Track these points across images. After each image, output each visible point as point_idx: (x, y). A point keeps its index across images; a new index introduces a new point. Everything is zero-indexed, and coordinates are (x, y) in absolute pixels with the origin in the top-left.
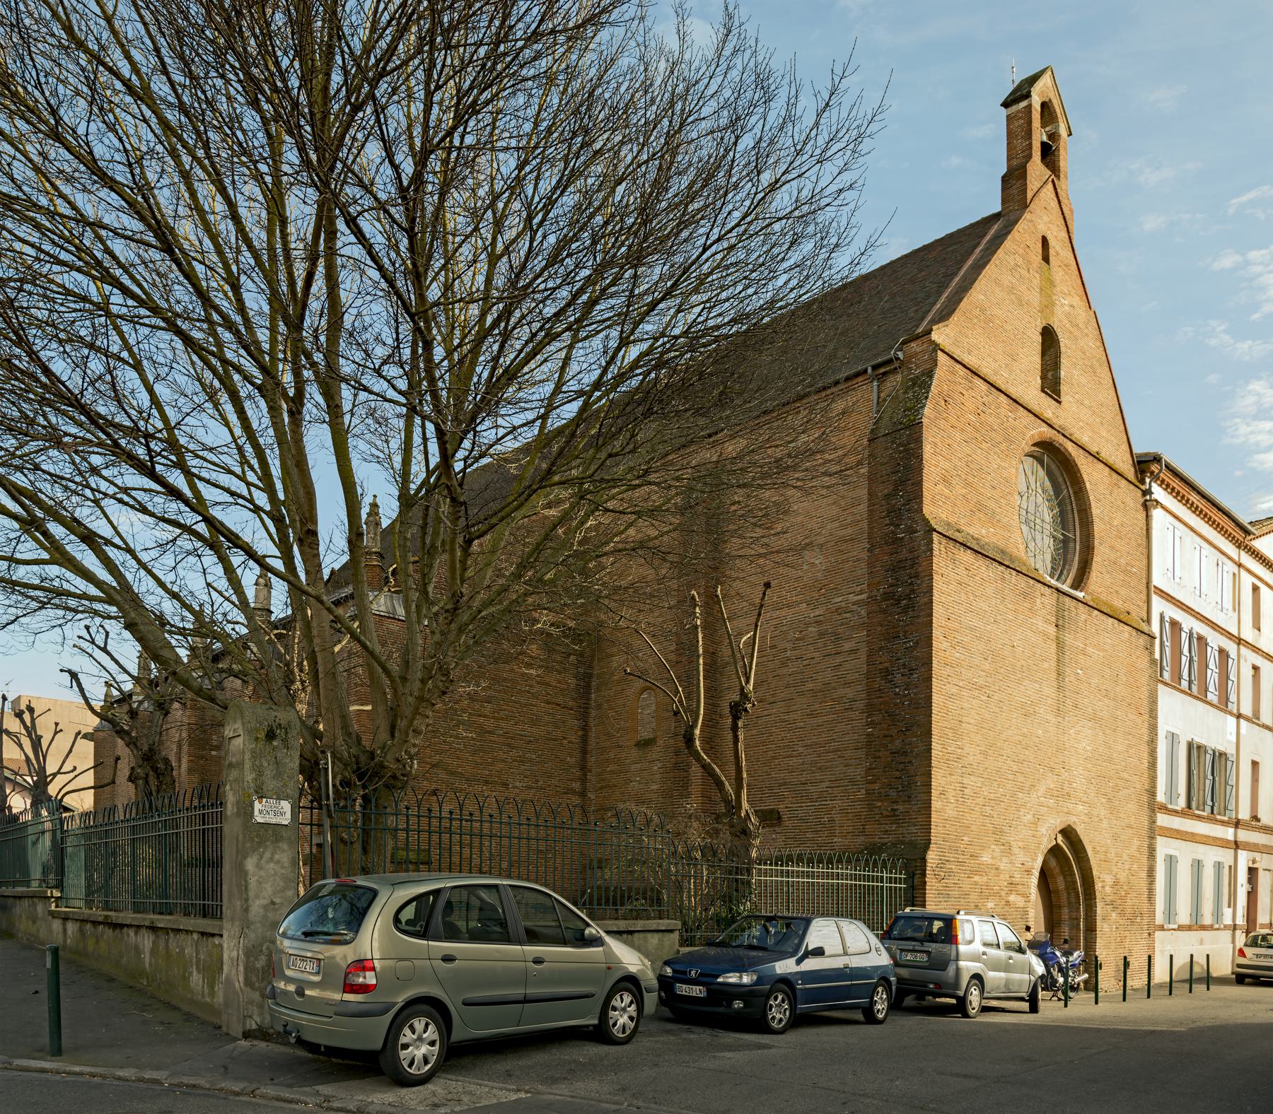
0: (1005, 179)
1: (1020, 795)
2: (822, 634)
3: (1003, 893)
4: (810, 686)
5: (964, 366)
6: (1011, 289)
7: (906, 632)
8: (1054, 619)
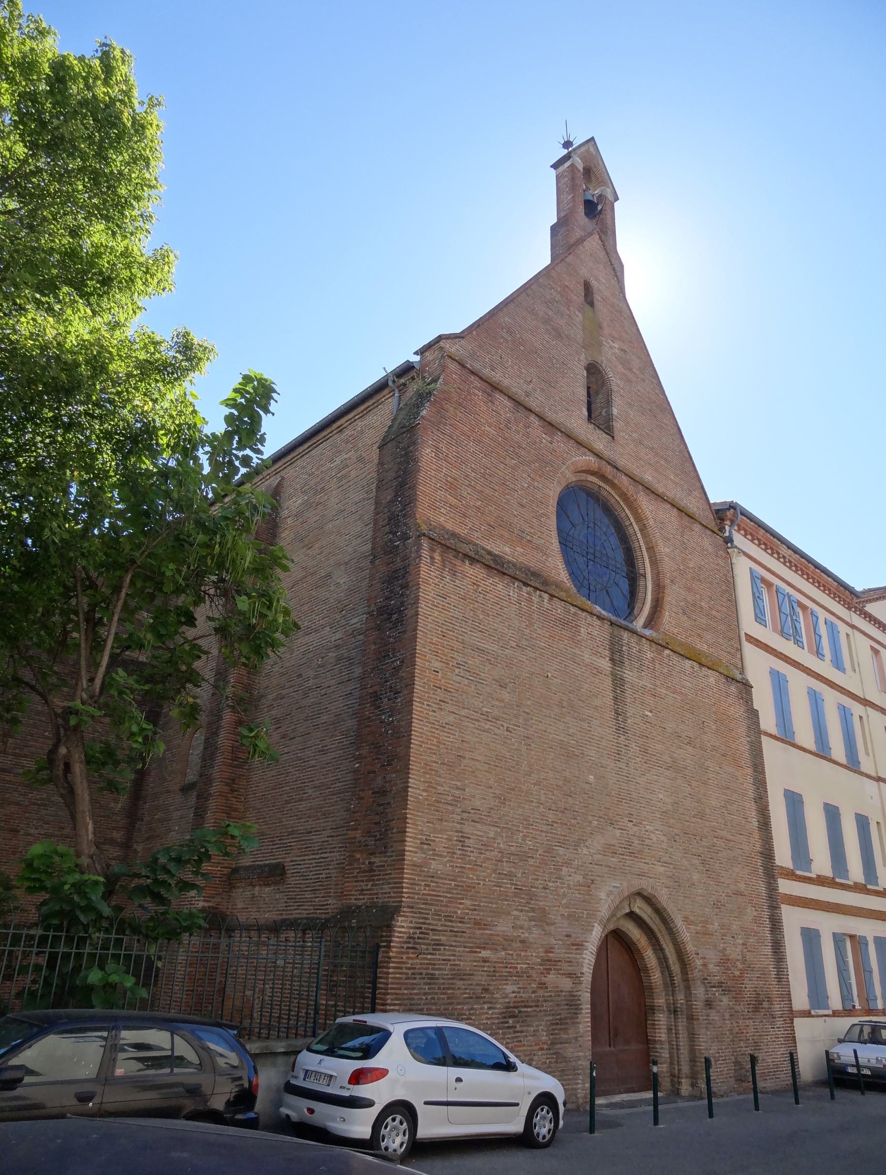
0: (554, 229)
1: (561, 851)
2: (339, 659)
3: (533, 973)
4: (324, 718)
5: (481, 378)
6: (547, 321)
7: (394, 650)
8: (607, 653)
